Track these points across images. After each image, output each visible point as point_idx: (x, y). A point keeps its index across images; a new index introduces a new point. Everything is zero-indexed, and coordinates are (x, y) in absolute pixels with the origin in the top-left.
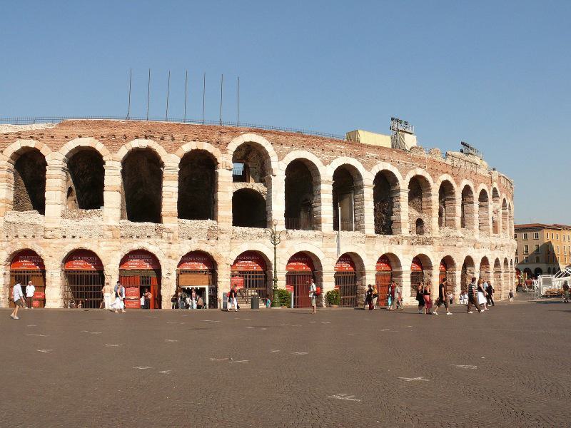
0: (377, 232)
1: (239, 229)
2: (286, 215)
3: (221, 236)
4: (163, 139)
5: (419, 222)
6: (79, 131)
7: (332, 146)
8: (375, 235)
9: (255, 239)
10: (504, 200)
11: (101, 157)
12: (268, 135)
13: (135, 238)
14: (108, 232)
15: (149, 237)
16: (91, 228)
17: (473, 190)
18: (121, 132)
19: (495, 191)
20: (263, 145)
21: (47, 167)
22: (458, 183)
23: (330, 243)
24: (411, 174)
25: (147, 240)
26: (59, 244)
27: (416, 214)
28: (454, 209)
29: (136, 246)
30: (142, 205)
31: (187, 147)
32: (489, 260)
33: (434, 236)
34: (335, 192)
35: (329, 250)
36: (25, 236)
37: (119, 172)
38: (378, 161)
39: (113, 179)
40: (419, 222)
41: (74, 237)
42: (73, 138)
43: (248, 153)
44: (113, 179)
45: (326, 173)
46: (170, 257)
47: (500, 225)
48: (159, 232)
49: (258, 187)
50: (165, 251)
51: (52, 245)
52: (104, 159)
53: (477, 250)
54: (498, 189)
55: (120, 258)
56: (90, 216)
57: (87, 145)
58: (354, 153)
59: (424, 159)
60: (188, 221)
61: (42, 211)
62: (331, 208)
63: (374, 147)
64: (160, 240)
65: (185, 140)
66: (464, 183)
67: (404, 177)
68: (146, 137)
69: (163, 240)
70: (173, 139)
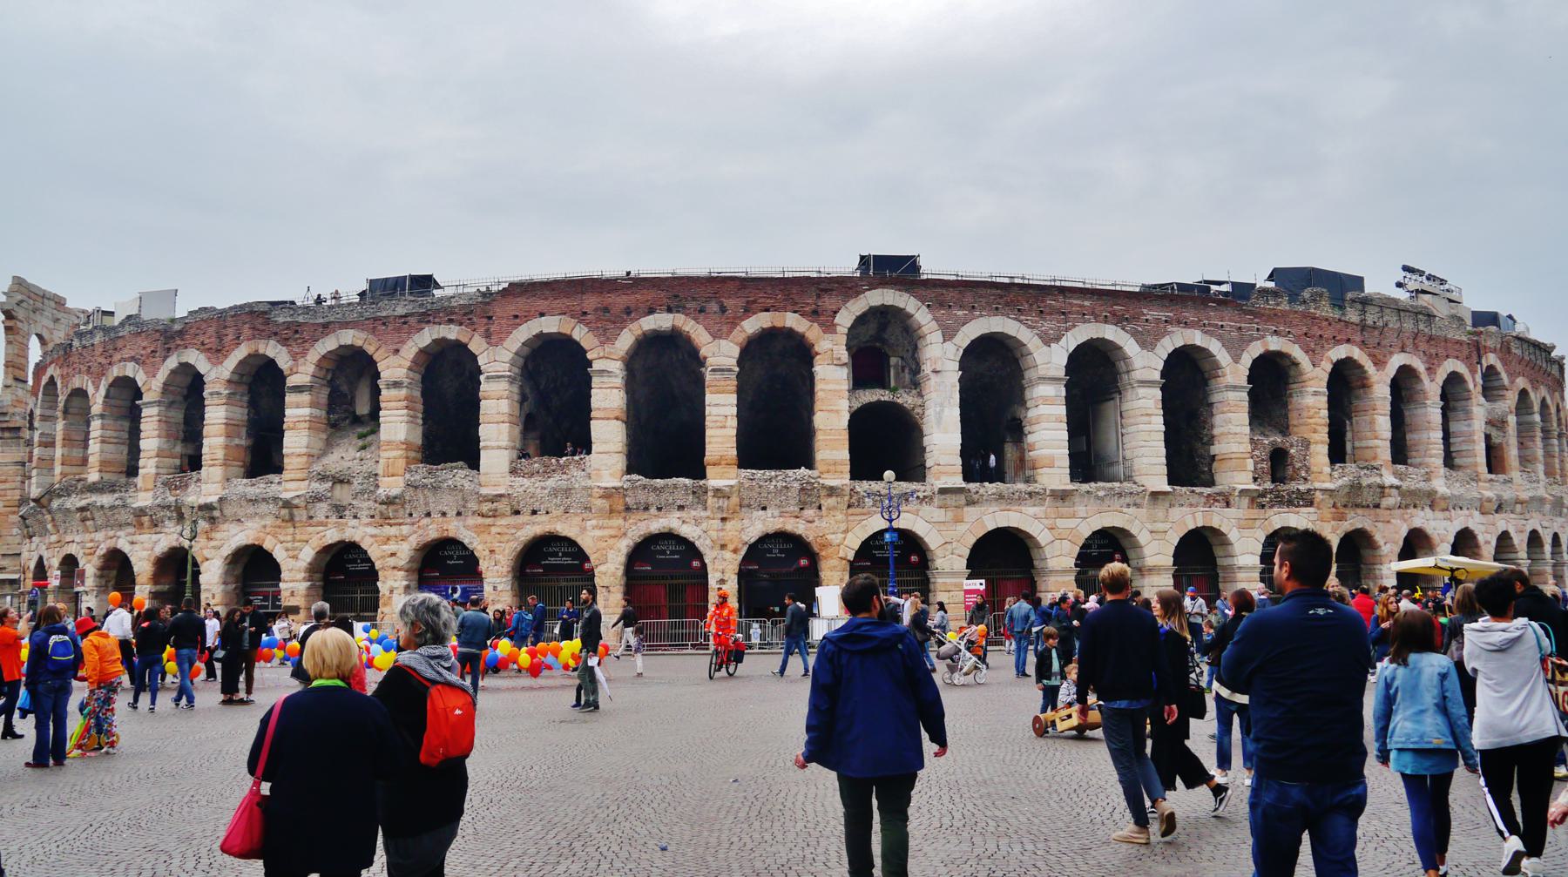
0: (1173, 479)
1: (863, 486)
2: (963, 454)
4: (701, 311)
6: (542, 304)
8: (1168, 488)
10: (1523, 394)
11: (585, 352)
13: (653, 510)
14: (598, 502)
15: (681, 508)
16: (568, 491)
19: (1490, 373)
20: (910, 309)
21: (482, 378)
22: (1379, 363)
23: (1063, 510)
24: (1255, 350)
25: (678, 514)
26: (508, 526)
28: (1372, 422)
29: (657, 525)
30: (665, 445)
31: (754, 324)
32: (1481, 538)
33: (1317, 485)
34: (1070, 401)
35: (1060, 523)
36: (444, 514)
37: (619, 381)
38: (1170, 328)
39: (608, 397)
41: (534, 512)
42: (527, 318)
43: (883, 327)
44: (608, 397)
46: (723, 547)
47: (1512, 452)
48: (700, 495)
49: (906, 399)
50: (714, 534)
51: (494, 530)
52: (589, 356)
53: (1439, 514)
54: (1499, 367)
55: (625, 551)
56: (563, 469)
57: (554, 330)
58: (1114, 314)
59: (1284, 314)
60: (759, 473)
61: (474, 463)
62: (1065, 435)
63: (1162, 297)
64: (704, 514)
65: (748, 311)
66: (1397, 361)
67: (1236, 359)
68: (670, 310)
69: (708, 513)
70: (723, 309)
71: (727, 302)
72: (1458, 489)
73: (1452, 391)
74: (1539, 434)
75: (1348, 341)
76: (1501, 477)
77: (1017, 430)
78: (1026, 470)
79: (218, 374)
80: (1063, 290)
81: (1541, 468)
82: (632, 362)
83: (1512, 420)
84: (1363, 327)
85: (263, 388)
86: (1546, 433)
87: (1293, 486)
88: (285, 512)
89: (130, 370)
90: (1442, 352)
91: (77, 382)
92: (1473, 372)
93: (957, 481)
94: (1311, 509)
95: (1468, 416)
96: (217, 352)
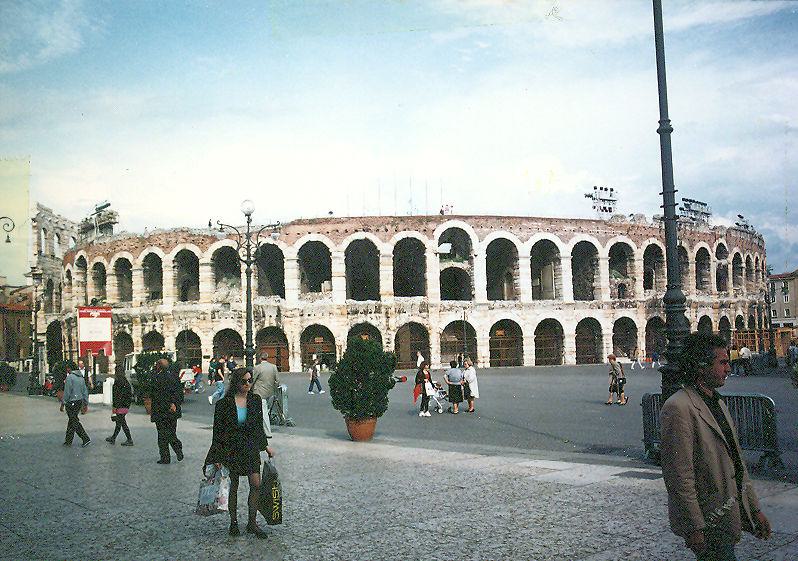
3: (430, 309)
5: (622, 288)
7: (530, 224)
9: (455, 311)
12: (469, 220)
16: (323, 307)
17: (688, 250)
18: (342, 228)
24: (611, 242)
27: (619, 280)
39: (339, 267)
40: (622, 288)
44: (339, 267)
45: (524, 250)
46: (388, 329)
49: (464, 265)
61: (283, 297)
67: (604, 246)
70: (387, 230)
71: (389, 227)
72: (702, 299)
77: (510, 278)
78: (514, 295)
79: (168, 259)
80: (527, 219)
82: (347, 253)
83: (730, 267)
85: (188, 264)
87: (628, 300)
88: (202, 316)
89: (126, 255)
90: (696, 239)
91: (98, 259)
93: (486, 301)
96: (167, 248)
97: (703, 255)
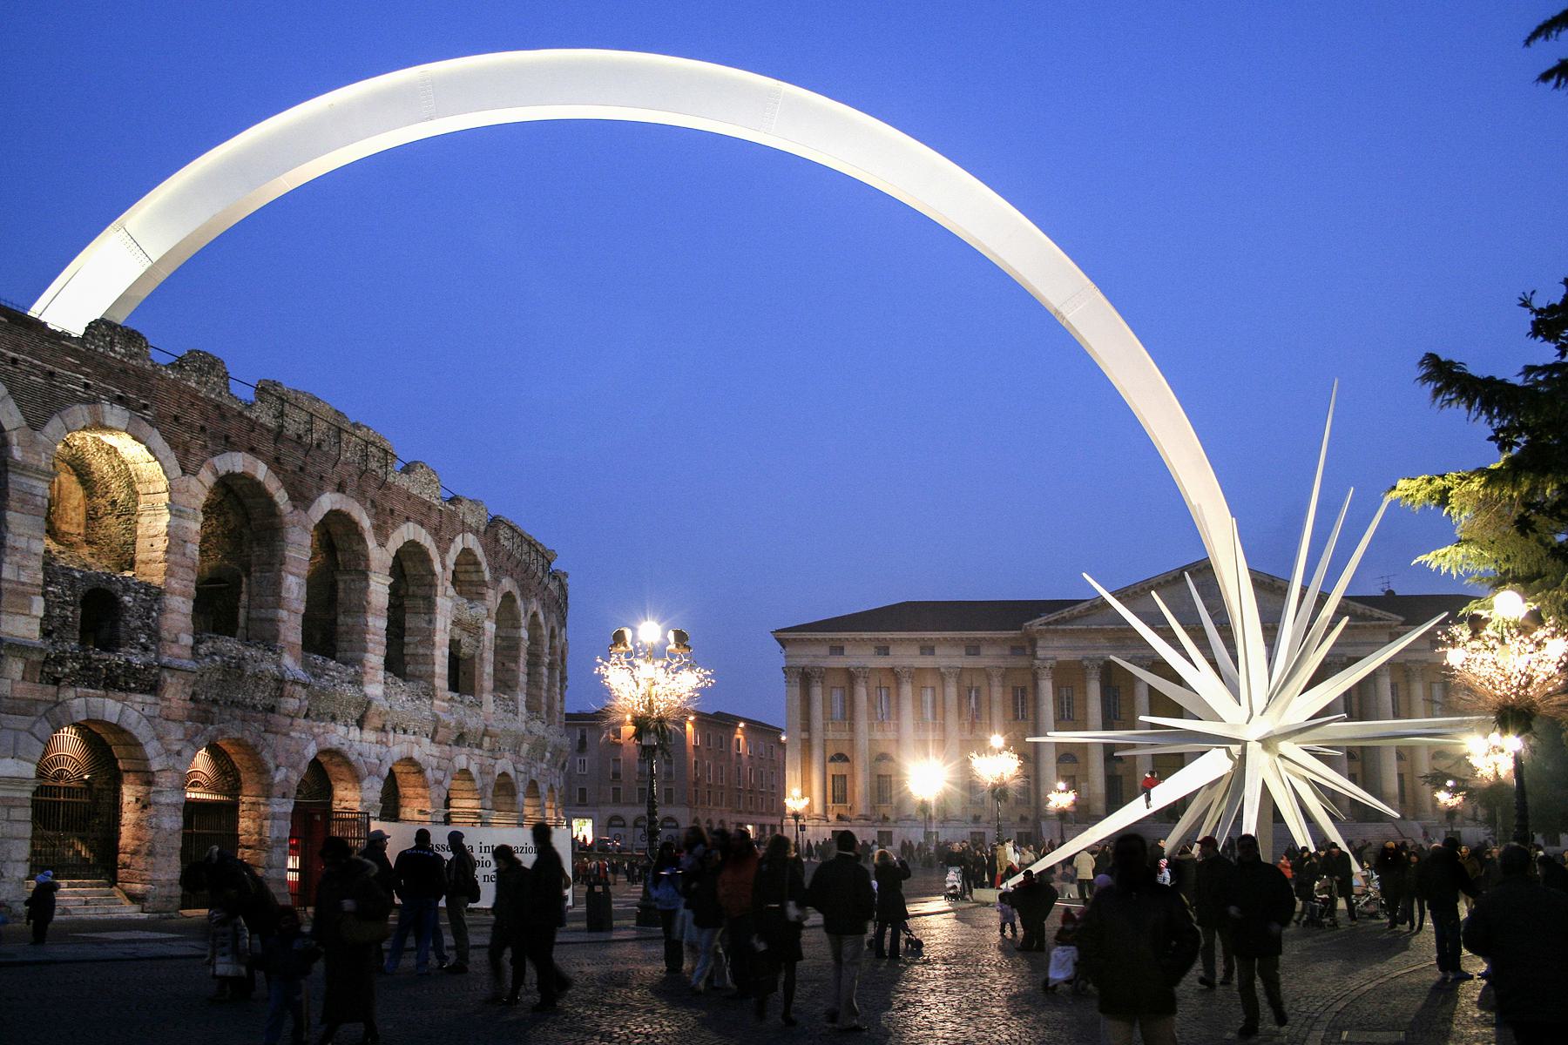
10: (508, 597)
28: (277, 583)
54: (479, 552)
66: (328, 502)
73: (410, 572)
74: (523, 657)
75: (252, 450)
76: (468, 699)
81: (521, 697)
83: (490, 627)
84: (279, 435)
86: (534, 663)
87: (118, 658)
92: (444, 551)
94: (149, 699)
95: (430, 607)
97: (410, 572)
